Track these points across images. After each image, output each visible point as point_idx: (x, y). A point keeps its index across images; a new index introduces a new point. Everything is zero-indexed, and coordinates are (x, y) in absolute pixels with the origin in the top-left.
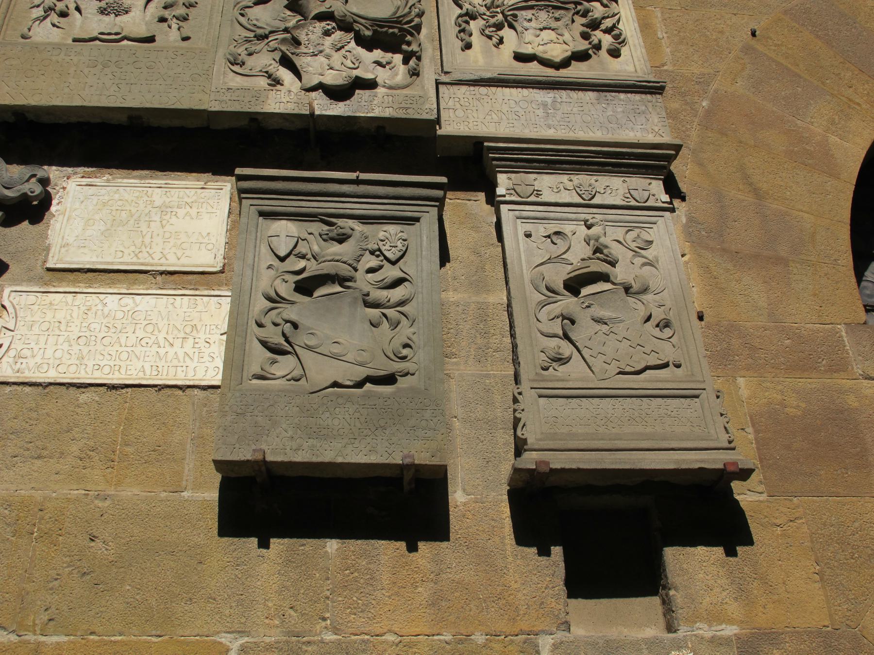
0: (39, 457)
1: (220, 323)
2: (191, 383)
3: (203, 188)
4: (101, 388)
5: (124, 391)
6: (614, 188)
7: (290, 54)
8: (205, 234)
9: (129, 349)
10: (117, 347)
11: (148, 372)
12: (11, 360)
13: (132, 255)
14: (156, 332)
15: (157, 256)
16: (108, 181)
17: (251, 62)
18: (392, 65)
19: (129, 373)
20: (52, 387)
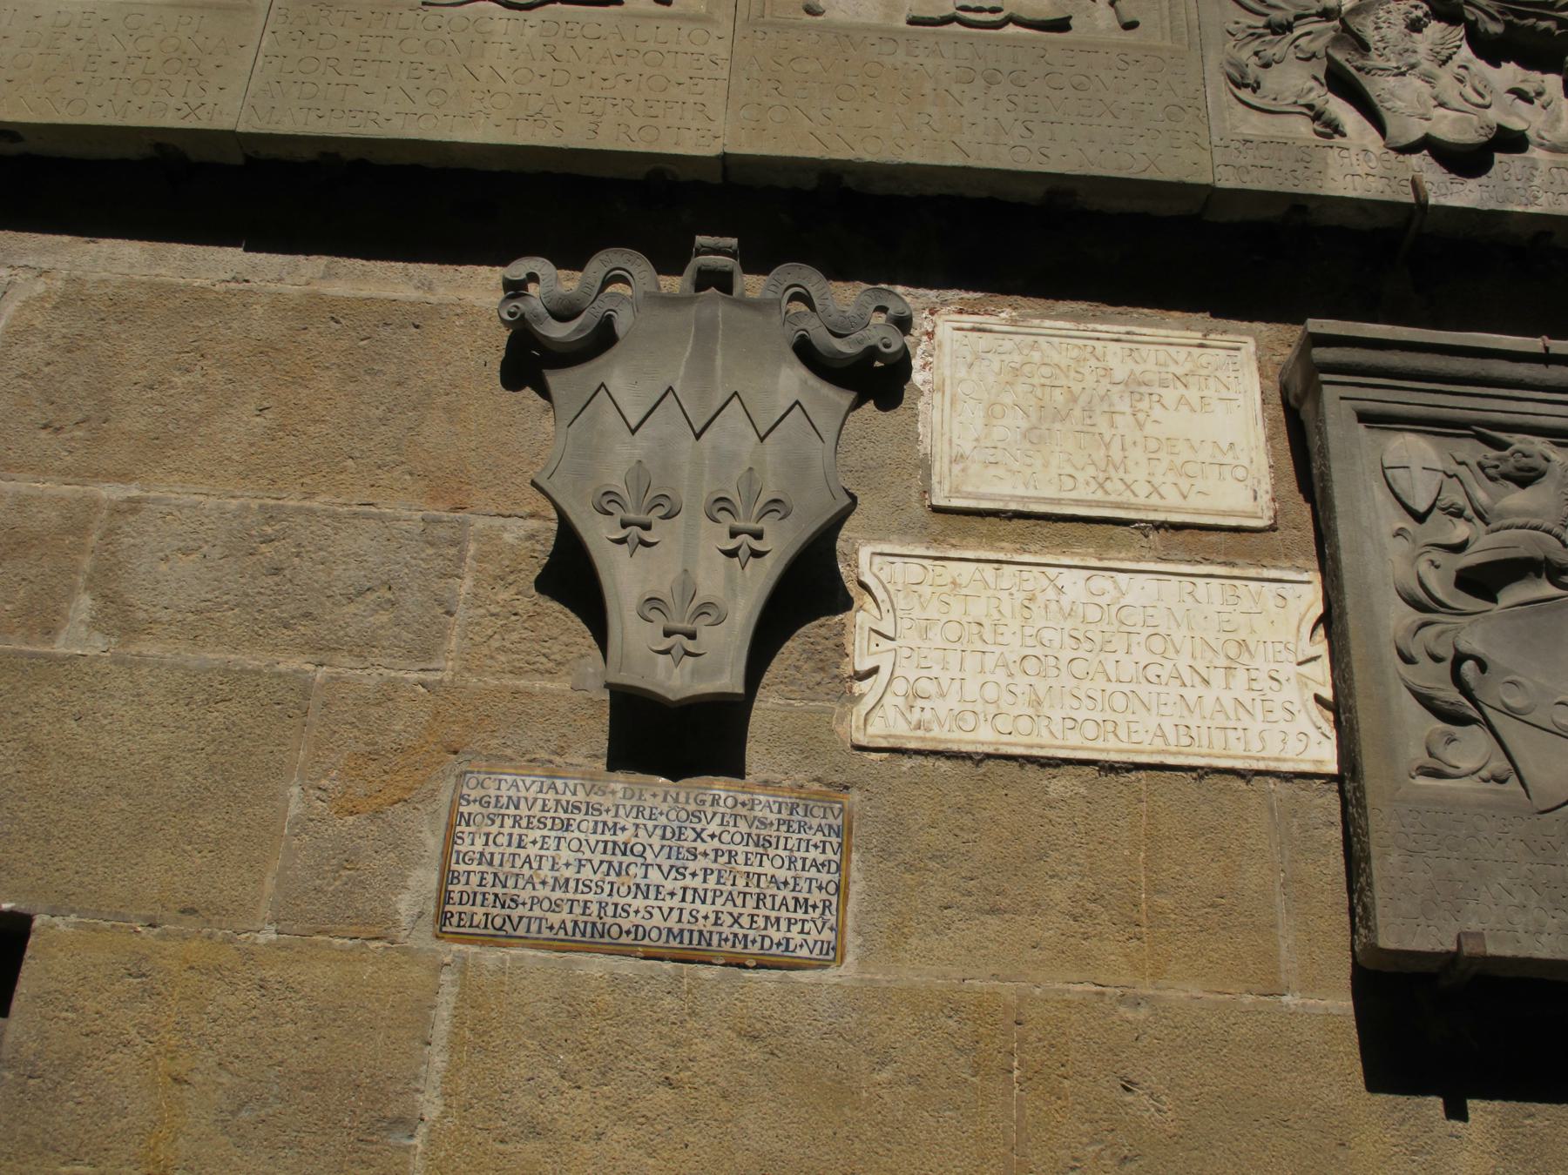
0: (993, 911)
1: (1293, 640)
2: (1261, 766)
3: (1201, 346)
4: (1087, 769)
5: (1133, 776)
7: (1353, 71)
8: (1225, 447)
9: (1126, 688)
10: (1100, 682)
11: (1172, 739)
12: (900, 701)
13: (1094, 485)
14: (1171, 653)
15: (1142, 489)
16: (1013, 322)
17: (1270, 79)
18: (1544, 98)
19: (1135, 738)
20: (991, 763)
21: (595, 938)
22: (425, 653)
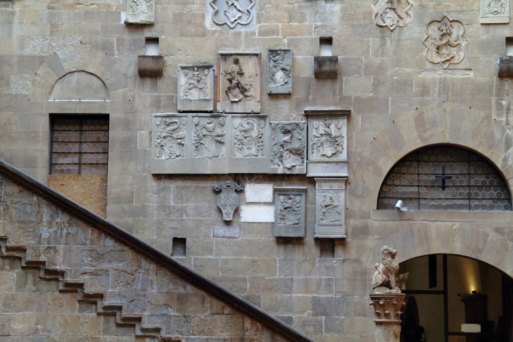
6: (336, 186)
21: (224, 237)
22: (210, 217)
